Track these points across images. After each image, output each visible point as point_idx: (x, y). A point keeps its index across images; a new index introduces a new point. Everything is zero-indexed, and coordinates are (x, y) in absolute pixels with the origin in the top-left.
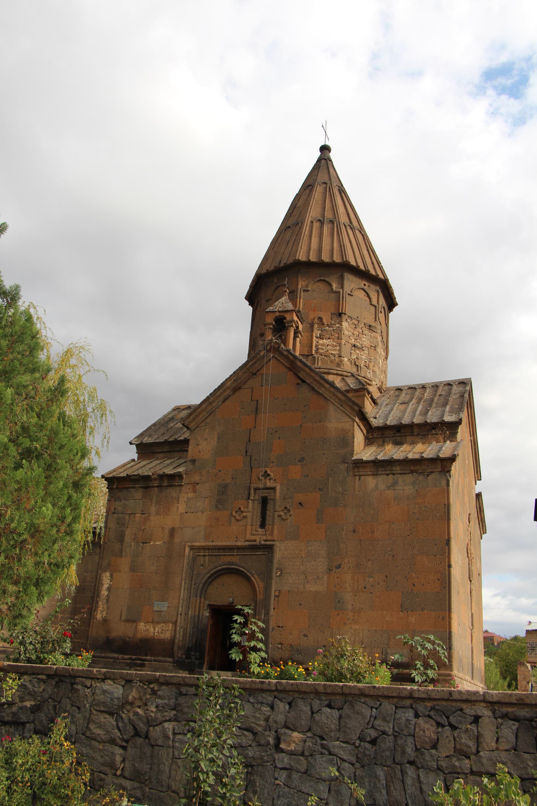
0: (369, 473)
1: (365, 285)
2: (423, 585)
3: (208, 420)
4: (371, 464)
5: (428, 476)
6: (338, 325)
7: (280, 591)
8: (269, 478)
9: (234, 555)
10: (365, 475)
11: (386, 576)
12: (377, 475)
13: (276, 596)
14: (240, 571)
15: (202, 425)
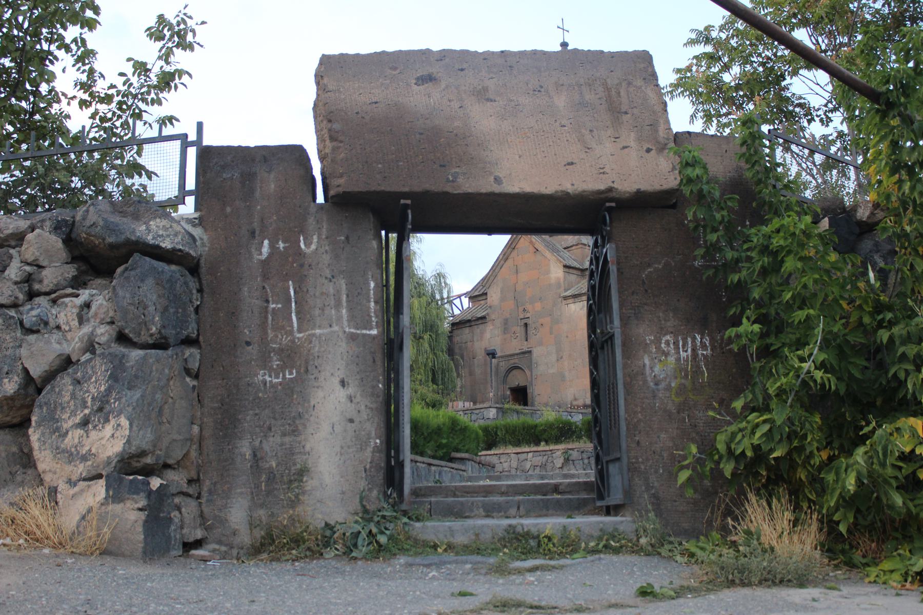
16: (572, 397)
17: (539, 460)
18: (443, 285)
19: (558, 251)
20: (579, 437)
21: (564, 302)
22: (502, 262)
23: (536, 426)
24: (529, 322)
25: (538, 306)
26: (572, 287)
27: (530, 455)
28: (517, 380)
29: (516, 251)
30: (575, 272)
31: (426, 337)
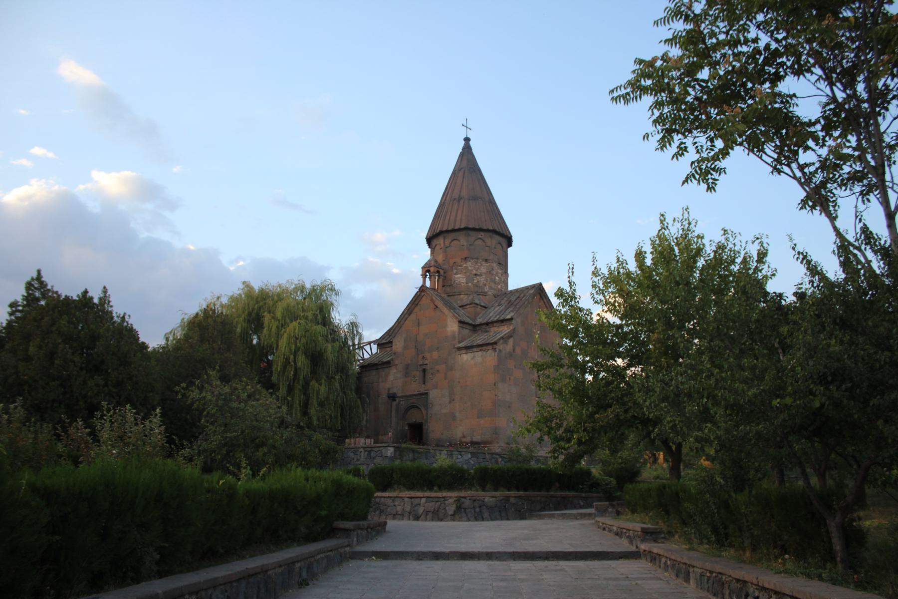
16: (462, 435)
17: (432, 506)
18: (355, 332)
19: (454, 309)
20: (471, 486)
21: (458, 352)
22: (406, 316)
23: (430, 471)
24: (428, 368)
25: (435, 355)
26: (465, 340)
27: (423, 500)
28: (414, 417)
29: (418, 307)
30: (468, 327)
31: (337, 377)
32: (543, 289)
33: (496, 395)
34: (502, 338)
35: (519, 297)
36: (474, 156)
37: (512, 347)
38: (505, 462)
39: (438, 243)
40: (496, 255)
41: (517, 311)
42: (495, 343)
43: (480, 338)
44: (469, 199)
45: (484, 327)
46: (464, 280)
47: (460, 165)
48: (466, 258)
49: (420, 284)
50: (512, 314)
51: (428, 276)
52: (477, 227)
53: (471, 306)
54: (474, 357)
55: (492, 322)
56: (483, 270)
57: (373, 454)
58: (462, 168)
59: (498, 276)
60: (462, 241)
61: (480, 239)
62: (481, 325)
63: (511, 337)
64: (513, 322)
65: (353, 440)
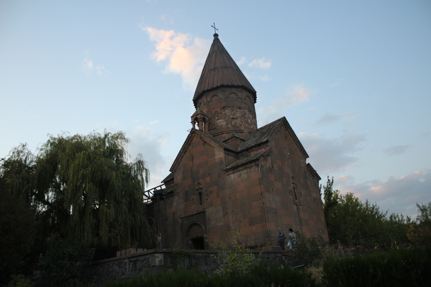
0: (231, 173)
1: (234, 91)
2: (255, 214)
3: (178, 167)
4: (231, 169)
5: (251, 168)
6: (224, 112)
7: (210, 228)
8: (200, 184)
9: (194, 218)
10: (230, 174)
11: (243, 213)
12: (234, 173)
13: (209, 230)
14: (197, 223)
15: (176, 170)
22: (183, 154)
30: (232, 154)
32: (287, 121)
33: (264, 204)
34: (262, 155)
35: (269, 129)
36: (222, 44)
37: (271, 164)
38: (288, 260)
39: (202, 101)
40: (246, 104)
41: (271, 135)
42: (257, 159)
43: (243, 160)
44: (222, 68)
45: (244, 153)
46: (225, 123)
47: (213, 50)
48: (224, 107)
49: (191, 126)
50: (267, 138)
51: (197, 123)
52: (230, 84)
53: (232, 139)
54: (240, 175)
55: (252, 148)
56: (238, 115)
57: (139, 265)
58: (215, 51)
59: (249, 119)
60: (219, 95)
61: (233, 93)
62: (242, 151)
63: (269, 155)
64: (269, 144)
65: (123, 251)
